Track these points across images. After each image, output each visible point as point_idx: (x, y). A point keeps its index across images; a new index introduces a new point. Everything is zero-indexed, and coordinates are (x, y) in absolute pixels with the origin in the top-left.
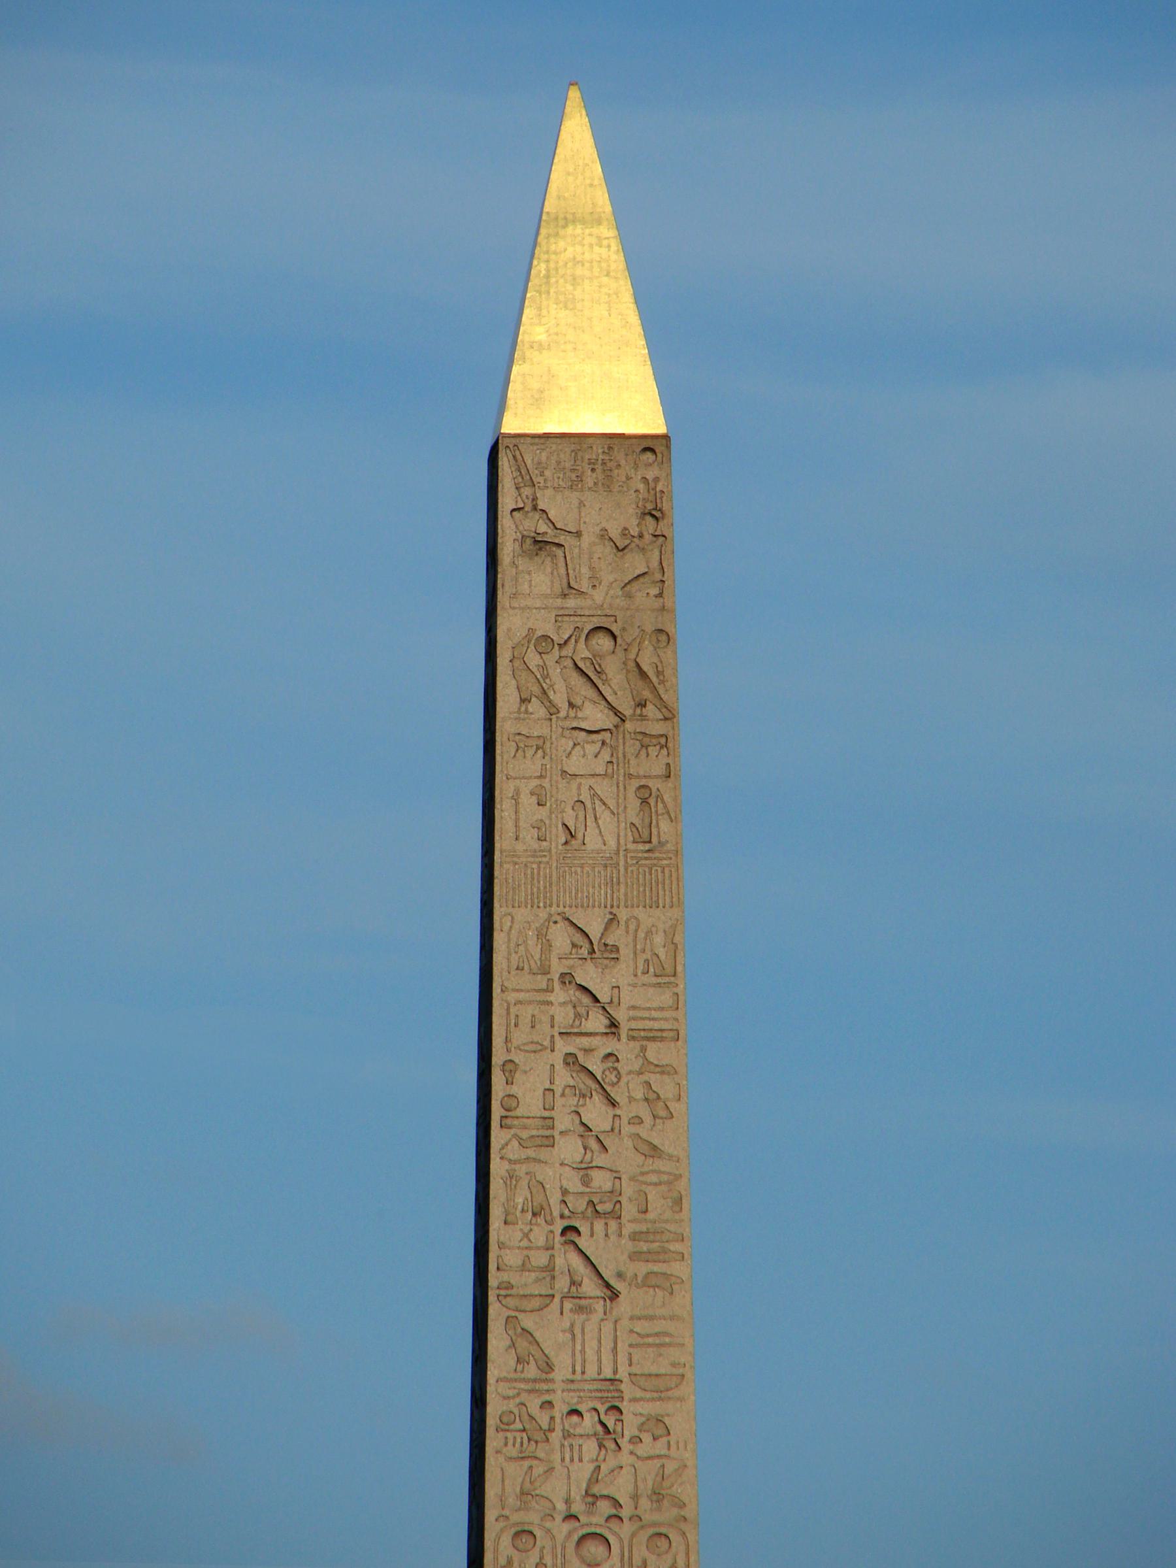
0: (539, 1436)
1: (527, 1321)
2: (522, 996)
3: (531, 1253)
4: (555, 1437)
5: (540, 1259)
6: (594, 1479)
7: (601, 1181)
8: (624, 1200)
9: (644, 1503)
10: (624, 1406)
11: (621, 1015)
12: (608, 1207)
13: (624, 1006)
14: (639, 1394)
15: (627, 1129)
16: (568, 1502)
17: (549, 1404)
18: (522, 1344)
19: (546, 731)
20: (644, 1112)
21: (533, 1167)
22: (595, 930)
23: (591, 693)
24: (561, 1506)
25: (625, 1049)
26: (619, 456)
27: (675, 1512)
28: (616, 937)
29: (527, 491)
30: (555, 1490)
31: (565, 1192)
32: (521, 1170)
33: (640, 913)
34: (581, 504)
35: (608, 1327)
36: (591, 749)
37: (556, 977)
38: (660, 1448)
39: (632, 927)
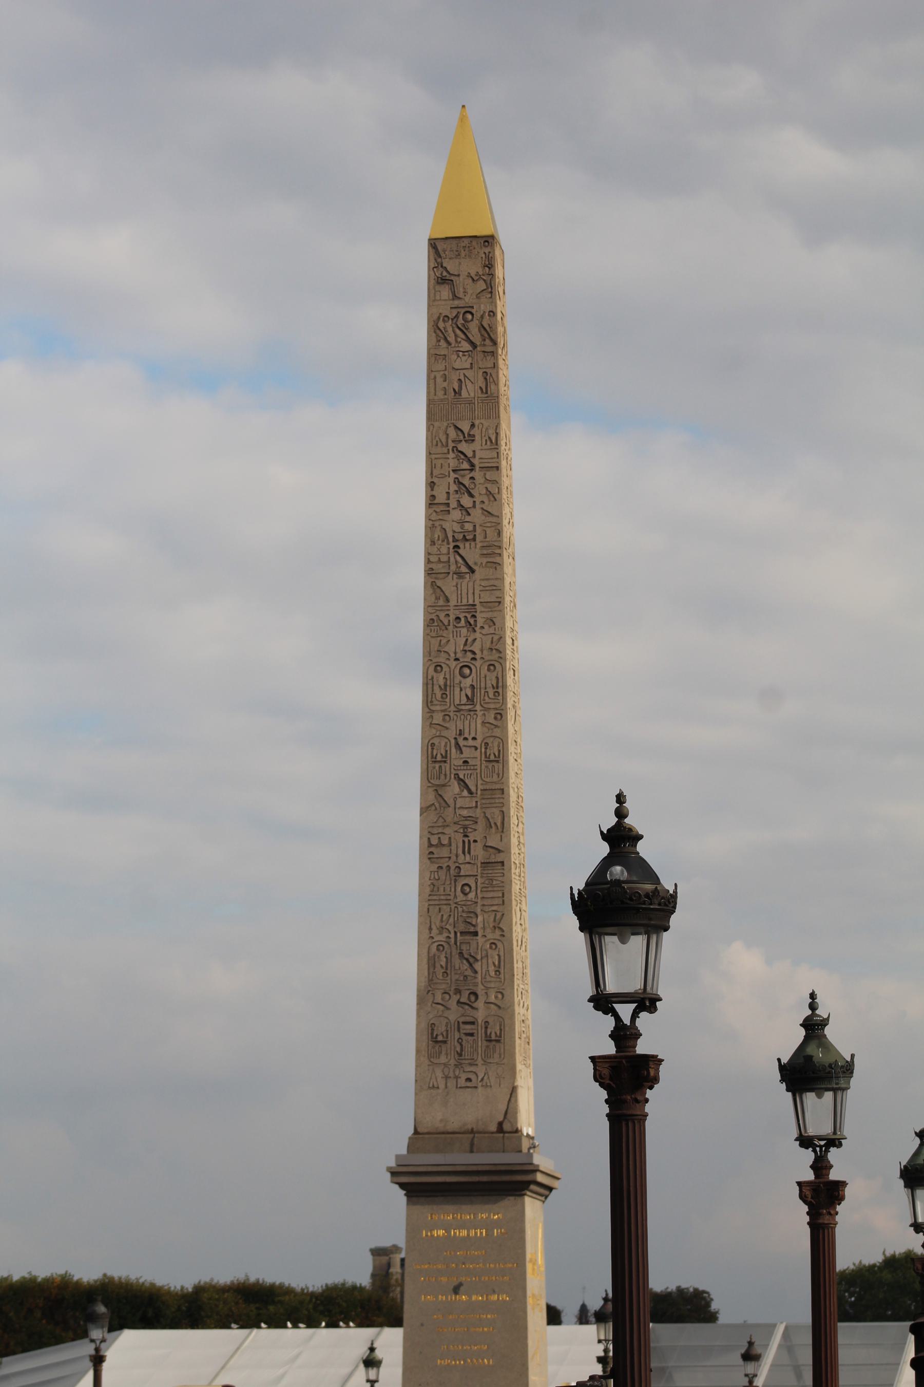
0: (444, 628)
1: (439, 583)
3: (441, 557)
4: (451, 628)
5: (444, 558)
6: (465, 644)
8: (477, 534)
9: (485, 652)
10: (477, 615)
11: (476, 461)
13: (477, 457)
14: (483, 609)
15: (478, 505)
16: (455, 653)
17: (448, 615)
18: (438, 591)
19: (446, 353)
20: (485, 499)
21: (441, 523)
22: (466, 431)
23: (463, 336)
24: (452, 655)
25: (477, 474)
26: (474, 243)
27: (498, 655)
28: (475, 431)
29: (439, 260)
30: (450, 648)
31: (454, 532)
32: (437, 524)
33: (483, 421)
34: (460, 264)
35: (471, 584)
36: (464, 358)
37: (451, 449)
39: (481, 426)
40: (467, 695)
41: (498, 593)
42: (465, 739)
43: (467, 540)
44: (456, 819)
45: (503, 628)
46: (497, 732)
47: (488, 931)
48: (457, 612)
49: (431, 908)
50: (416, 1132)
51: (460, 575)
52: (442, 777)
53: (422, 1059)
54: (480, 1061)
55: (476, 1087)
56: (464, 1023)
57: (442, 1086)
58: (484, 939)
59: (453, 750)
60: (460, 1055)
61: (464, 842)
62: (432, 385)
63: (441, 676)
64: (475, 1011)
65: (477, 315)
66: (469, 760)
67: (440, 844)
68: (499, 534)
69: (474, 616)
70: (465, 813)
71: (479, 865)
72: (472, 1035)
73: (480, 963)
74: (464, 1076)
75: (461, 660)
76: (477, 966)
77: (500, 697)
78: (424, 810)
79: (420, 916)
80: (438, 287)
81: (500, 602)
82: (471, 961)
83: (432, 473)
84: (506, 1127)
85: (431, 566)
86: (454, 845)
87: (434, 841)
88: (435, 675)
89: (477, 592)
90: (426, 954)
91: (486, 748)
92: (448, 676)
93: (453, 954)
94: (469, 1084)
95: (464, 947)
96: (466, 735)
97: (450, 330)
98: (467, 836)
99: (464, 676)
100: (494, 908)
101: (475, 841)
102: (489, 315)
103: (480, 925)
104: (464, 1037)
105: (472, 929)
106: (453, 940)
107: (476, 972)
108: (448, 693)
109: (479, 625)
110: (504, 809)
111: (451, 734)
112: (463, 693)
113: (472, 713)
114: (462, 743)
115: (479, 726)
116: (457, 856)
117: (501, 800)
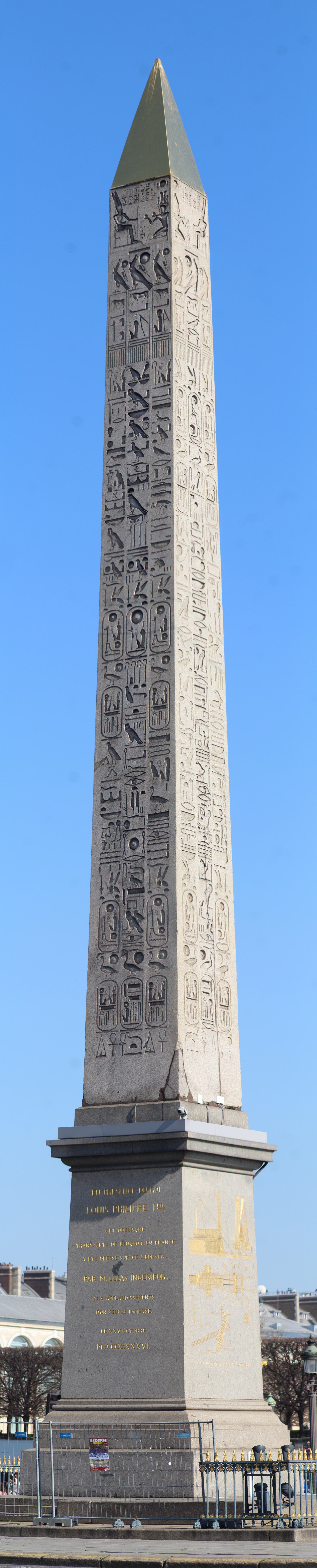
1: (115, 529)
2: (114, 402)
4: (124, 573)
5: (119, 504)
7: (142, 468)
10: (149, 557)
11: (150, 401)
12: (144, 478)
16: (128, 599)
20: (158, 437)
21: (118, 468)
24: (126, 601)
26: (152, 185)
27: (167, 595)
30: (124, 595)
31: (129, 475)
32: (114, 469)
33: (157, 359)
36: (140, 300)
38: (161, 571)
40: (138, 642)
41: (167, 532)
42: (136, 687)
43: (141, 482)
44: (126, 772)
45: (172, 567)
46: (165, 676)
47: (155, 885)
48: (131, 557)
49: (102, 866)
50: (84, 1103)
51: (134, 518)
52: (115, 728)
53: (92, 1026)
54: (144, 1026)
55: (140, 1053)
56: (131, 986)
57: (109, 1054)
58: (151, 895)
59: (125, 700)
60: (126, 1020)
61: (133, 794)
62: (111, 332)
63: (116, 624)
64: (140, 972)
65: (153, 255)
66: (138, 708)
67: (112, 800)
68: (170, 471)
69: (145, 559)
70: (134, 764)
71: (147, 817)
72: (137, 998)
73: (145, 921)
74: (129, 1042)
75: (133, 605)
76: (143, 924)
77: (168, 639)
78: (98, 765)
79: (92, 876)
80: (118, 235)
81: (168, 541)
82: (136, 919)
83: (110, 420)
84: (168, 1094)
85: (107, 513)
86: (123, 798)
87: (106, 797)
88: (110, 623)
89: (149, 533)
90: (97, 915)
91: (154, 694)
92: (121, 624)
93: (122, 913)
94: (134, 1050)
95: (131, 905)
96: (137, 683)
97: (129, 274)
98: (136, 788)
99: (135, 622)
100: (160, 861)
101: (143, 793)
102: (165, 254)
103: (146, 881)
104: (130, 1002)
105: (139, 886)
106: (121, 899)
107: (142, 931)
108: (121, 641)
109: (150, 568)
110: (169, 756)
111: (122, 683)
112: (135, 639)
113: (142, 659)
114: (133, 691)
115: (149, 671)
116: (126, 810)
117: (167, 747)
